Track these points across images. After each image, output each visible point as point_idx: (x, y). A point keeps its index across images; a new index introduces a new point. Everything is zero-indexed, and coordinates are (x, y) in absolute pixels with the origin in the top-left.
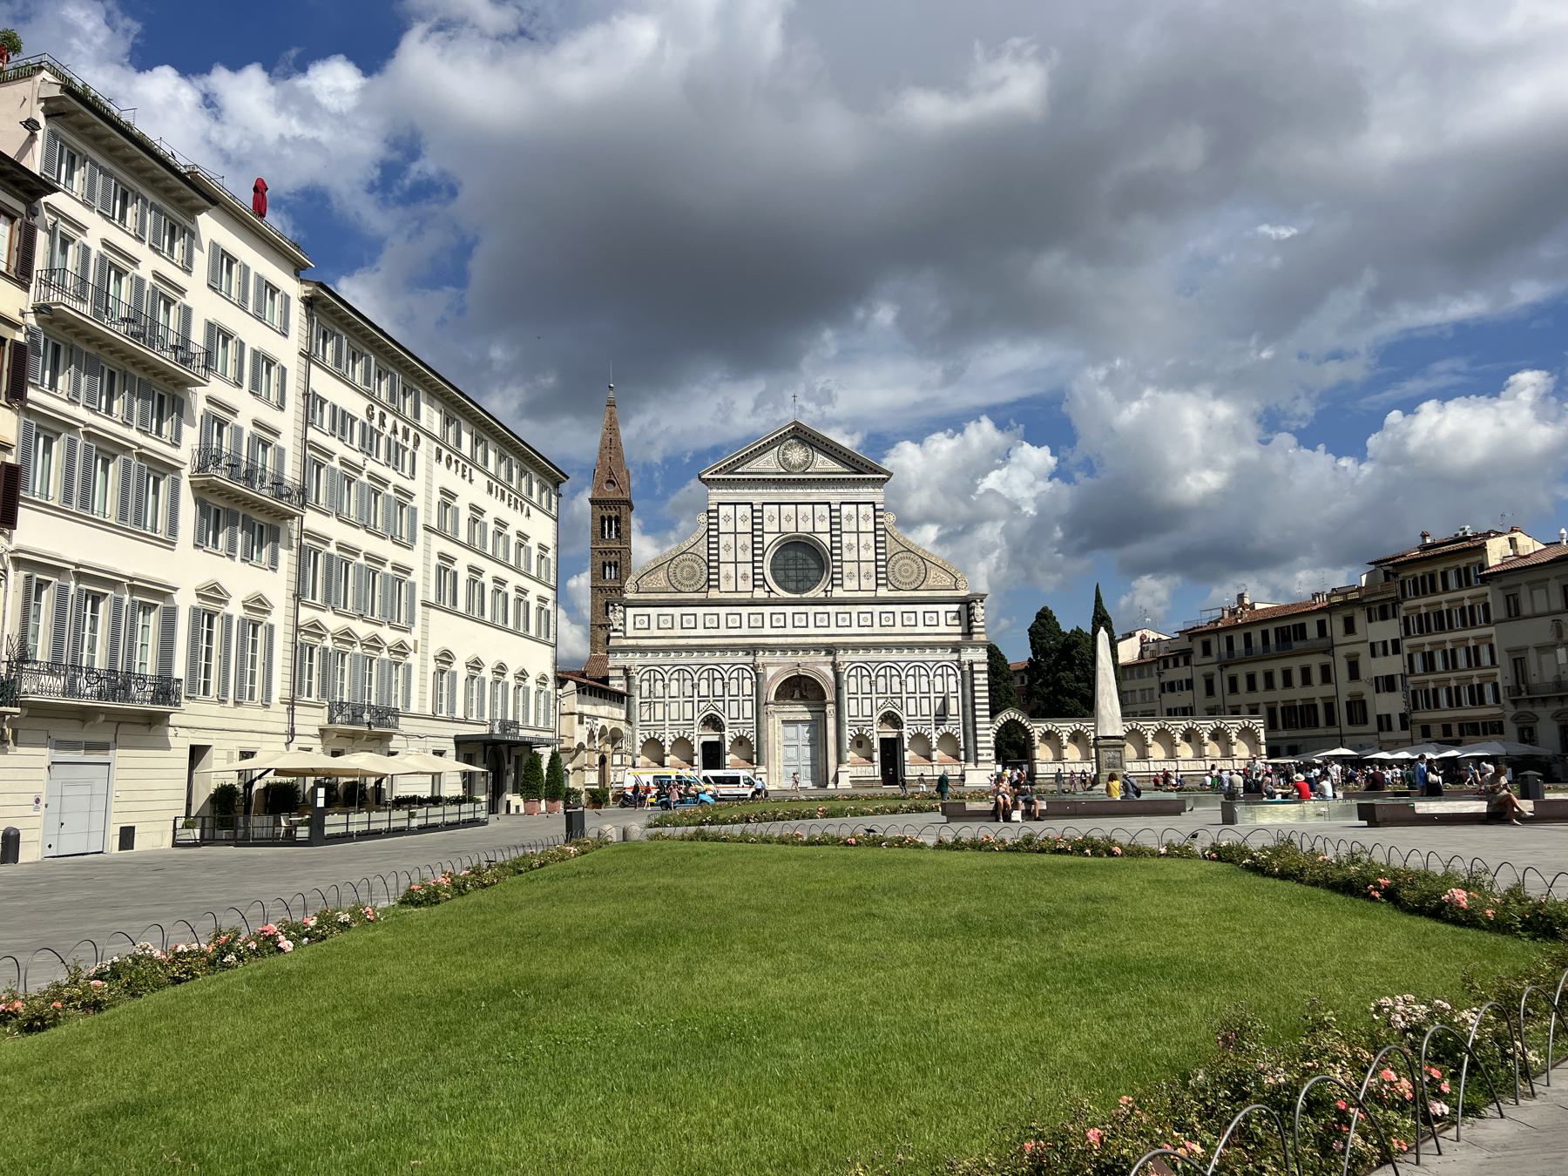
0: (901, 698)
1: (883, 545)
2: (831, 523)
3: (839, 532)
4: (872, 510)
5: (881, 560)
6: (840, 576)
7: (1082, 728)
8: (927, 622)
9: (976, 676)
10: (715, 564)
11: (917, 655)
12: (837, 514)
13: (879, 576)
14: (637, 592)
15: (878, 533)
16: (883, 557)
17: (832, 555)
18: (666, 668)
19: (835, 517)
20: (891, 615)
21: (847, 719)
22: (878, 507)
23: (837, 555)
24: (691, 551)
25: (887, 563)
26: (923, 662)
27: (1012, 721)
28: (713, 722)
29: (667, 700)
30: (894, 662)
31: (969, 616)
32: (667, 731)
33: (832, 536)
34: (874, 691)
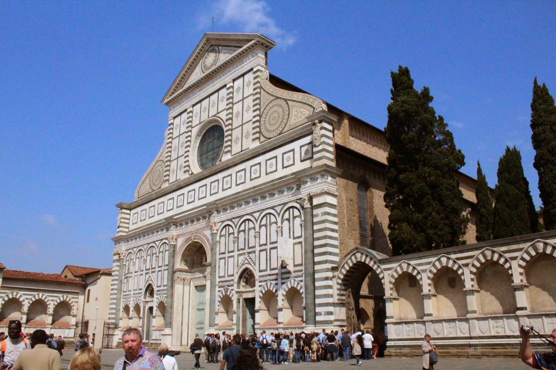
0: (254, 252)
7: (450, 265)
9: (315, 212)
10: (168, 163)
11: (269, 202)
14: (139, 198)
16: (258, 112)
18: (135, 249)
21: (218, 280)
23: (228, 125)
24: (160, 159)
26: (272, 208)
27: (359, 262)
28: (150, 290)
29: (134, 274)
30: (251, 214)
32: (132, 299)
34: (236, 249)
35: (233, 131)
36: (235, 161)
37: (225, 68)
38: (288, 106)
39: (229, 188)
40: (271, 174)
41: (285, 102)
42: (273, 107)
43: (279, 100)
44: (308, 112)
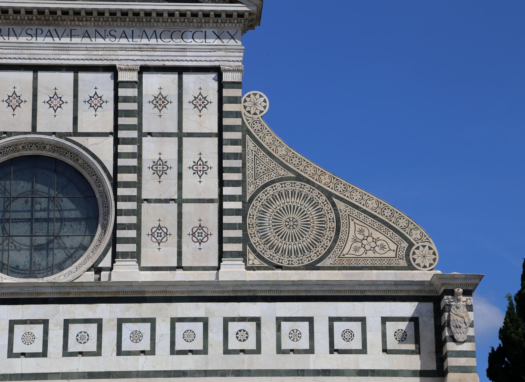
1: (238, 163)
2: (117, 114)
3: (134, 134)
4: (215, 85)
5: (232, 198)
6: (132, 234)
8: (339, 344)
12: (132, 92)
13: (227, 233)
15: (227, 135)
16: (237, 191)
17: (115, 185)
19: (126, 99)
20: (251, 327)
22: (227, 77)
23: (127, 185)
25: (247, 204)
31: (439, 329)
33: (117, 142)
35: (145, 205)
36: (170, 292)
38: (336, 211)
39: (143, 352)
40: (292, 354)
41: (324, 198)
42: (287, 195)
43: (308, 186)
44: (393, 247)
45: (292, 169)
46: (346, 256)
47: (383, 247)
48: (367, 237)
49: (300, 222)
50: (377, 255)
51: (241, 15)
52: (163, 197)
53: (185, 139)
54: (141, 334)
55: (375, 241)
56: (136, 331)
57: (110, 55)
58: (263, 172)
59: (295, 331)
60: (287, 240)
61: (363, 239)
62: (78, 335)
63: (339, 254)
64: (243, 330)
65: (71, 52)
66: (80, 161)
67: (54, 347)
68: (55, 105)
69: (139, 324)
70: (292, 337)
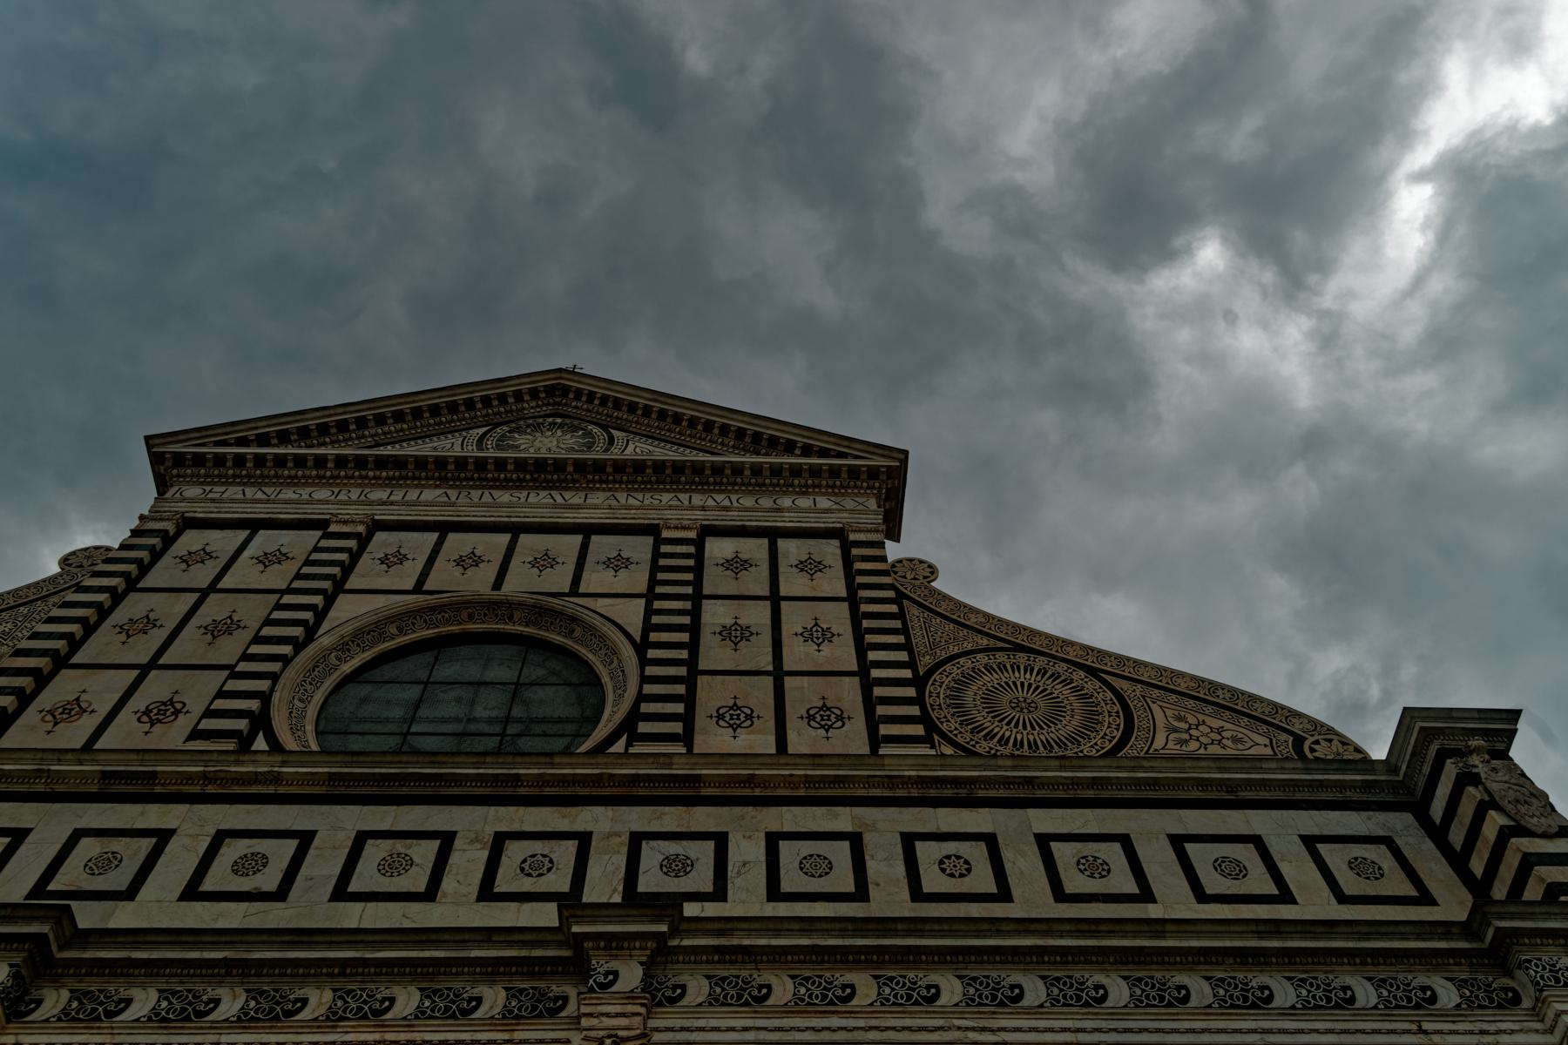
37: (659, 482)
43: (1042, 658)
45: (1005, 639)
46: (1161, 752)
47: (1236, 740)
48: (1197, 726)
49: (1041, 704)
50: (1229, 751)
51: (873, 473)
52: (742, 668)
53: (783, 604)
54: (689, 862)
55: (1219, 731)
56: (677, 855)
57: (650, 514)
58: (946, 641)
59: (1091, 859)
60: (1020, 727)
61: (1190, 728)
62: (524, 861)
63: (1146, 749)
64: (955, 856)
65: (581, 511)
66: (578, 632)
67: (458, 881)
68: (542, 566)
69: (684, 843)
70: (1085, 870)
